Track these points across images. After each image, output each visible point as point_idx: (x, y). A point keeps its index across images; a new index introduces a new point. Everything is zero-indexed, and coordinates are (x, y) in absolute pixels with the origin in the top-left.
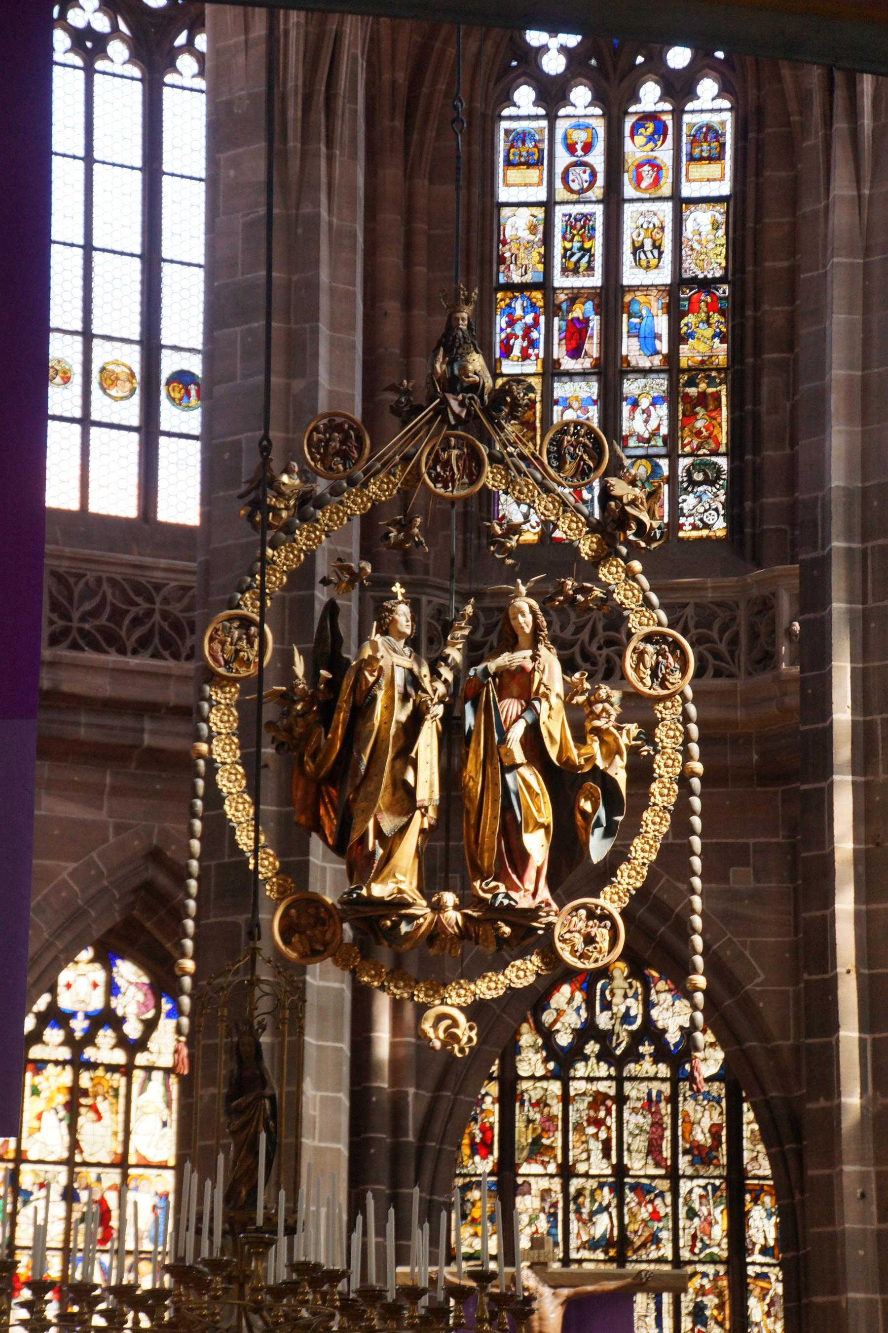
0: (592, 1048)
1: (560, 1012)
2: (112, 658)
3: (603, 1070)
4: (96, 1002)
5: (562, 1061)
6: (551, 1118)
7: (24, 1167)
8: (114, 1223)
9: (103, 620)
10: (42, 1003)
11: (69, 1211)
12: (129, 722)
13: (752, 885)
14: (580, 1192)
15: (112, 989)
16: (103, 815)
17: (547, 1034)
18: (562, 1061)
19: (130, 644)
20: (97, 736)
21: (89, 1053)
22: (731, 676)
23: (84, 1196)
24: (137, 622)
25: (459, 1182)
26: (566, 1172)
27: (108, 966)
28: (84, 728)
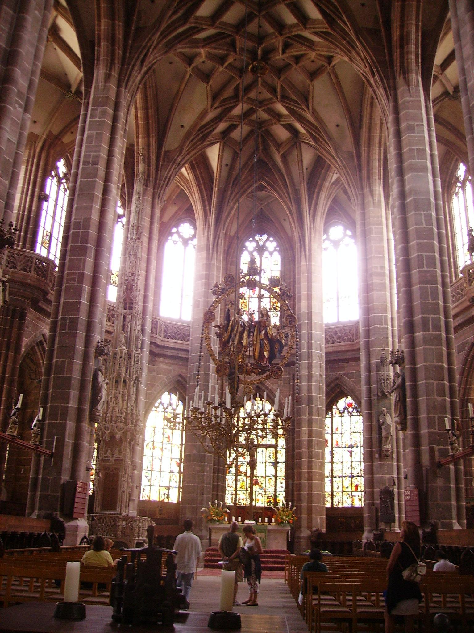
2: (174, 341)
8: (171, 439)
9: (173, 334)
10: (159, 401)
12: (176, 352)
16: (171, 368)
19: (177, 338)
24: (179, 335)
28: (169, 352)
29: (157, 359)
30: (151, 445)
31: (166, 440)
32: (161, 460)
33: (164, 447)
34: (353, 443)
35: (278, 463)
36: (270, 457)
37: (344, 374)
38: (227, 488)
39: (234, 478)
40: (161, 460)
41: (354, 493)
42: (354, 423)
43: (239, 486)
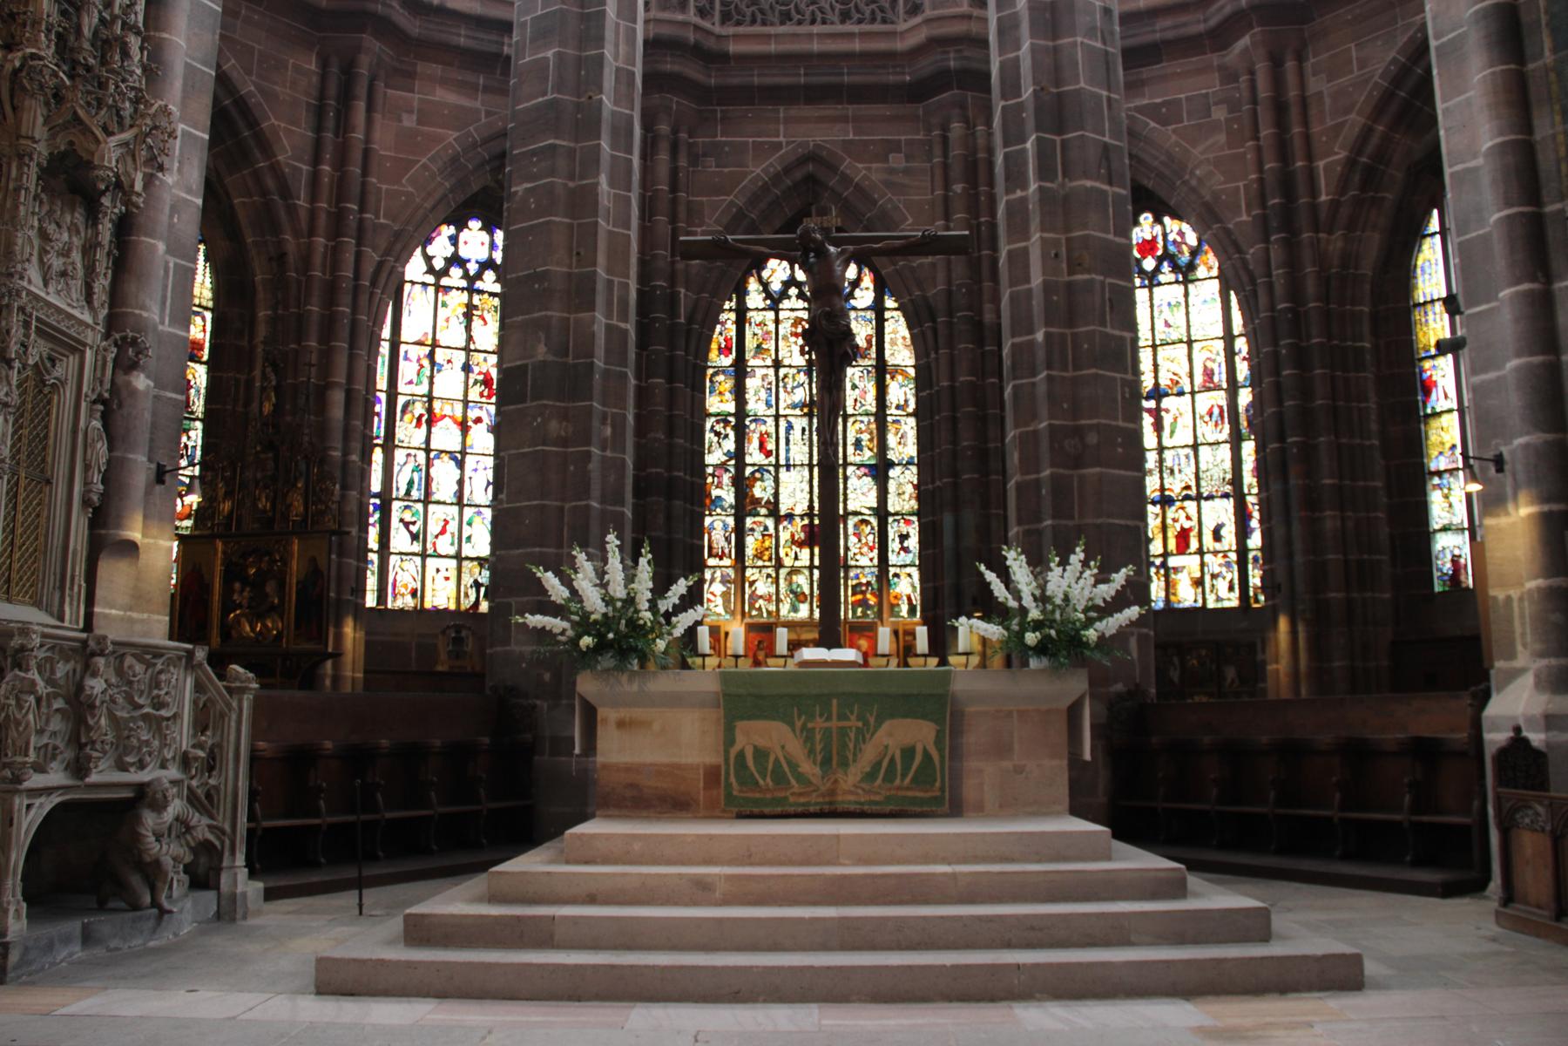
0: (793, 291)
1: (773, 271)
3: (801, 304)
4: (483, 255)
5: (774, 301)
6: (768, 333)
7: (438, 350)
11: (467, 378)
12: (494, 37)
13: (904, 164)
14: (786, 376)
15: (493, 246)
17: (765, 285)
18: (774, 301)
20: (471, 44)
21: (479, 285)
22: (892, 23)
23: (477, 370)
25: (710, 371)
26: (777, 364)
27: (491, 234)
28: (462, 38)
29: (421, 67)
30: (419, 409)
31: (474, 394)
32: (461, 465)
33: (473, 414)
34: (1164, 381)
35: (891, 464)
36: (858, 444)
37: (1139, 109)
38: (712, 562)
39: (731, 521)
40: (461, 465)
41: (1173, 562)
42: (1165, 308)
43: (750, 551)
